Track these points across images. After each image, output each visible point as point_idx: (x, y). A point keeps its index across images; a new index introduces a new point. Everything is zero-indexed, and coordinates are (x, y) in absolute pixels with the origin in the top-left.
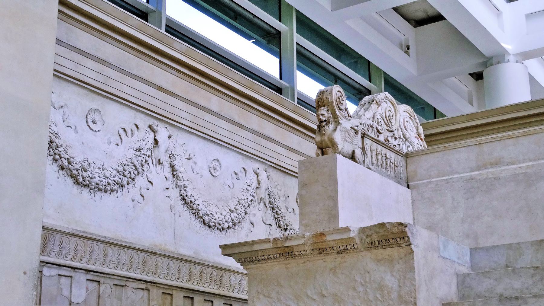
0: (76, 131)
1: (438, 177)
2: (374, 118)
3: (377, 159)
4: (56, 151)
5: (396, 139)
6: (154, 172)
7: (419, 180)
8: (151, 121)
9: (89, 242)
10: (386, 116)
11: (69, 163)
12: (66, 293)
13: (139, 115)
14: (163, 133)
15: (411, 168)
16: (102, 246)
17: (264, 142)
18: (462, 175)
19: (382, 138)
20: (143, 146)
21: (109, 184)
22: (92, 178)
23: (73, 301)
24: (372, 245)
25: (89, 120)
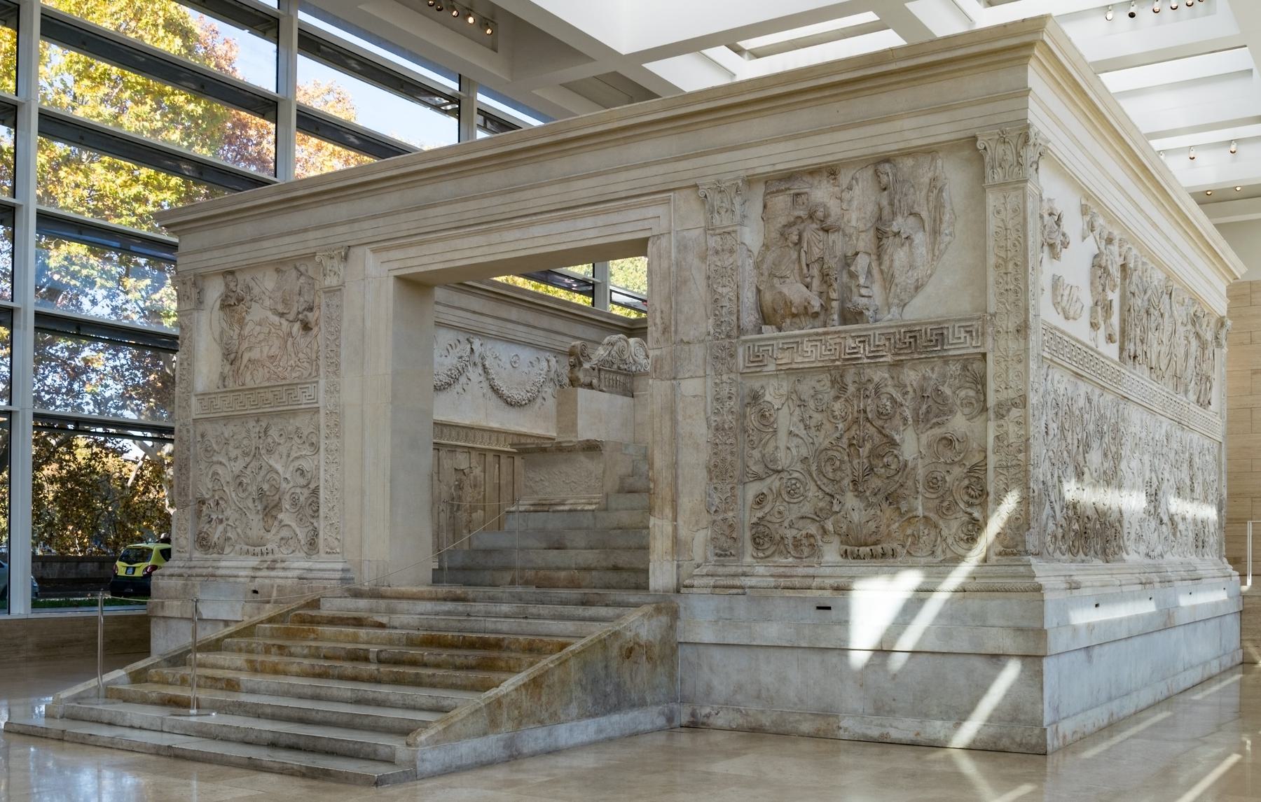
14: (477, 343)
17: (553, 336)
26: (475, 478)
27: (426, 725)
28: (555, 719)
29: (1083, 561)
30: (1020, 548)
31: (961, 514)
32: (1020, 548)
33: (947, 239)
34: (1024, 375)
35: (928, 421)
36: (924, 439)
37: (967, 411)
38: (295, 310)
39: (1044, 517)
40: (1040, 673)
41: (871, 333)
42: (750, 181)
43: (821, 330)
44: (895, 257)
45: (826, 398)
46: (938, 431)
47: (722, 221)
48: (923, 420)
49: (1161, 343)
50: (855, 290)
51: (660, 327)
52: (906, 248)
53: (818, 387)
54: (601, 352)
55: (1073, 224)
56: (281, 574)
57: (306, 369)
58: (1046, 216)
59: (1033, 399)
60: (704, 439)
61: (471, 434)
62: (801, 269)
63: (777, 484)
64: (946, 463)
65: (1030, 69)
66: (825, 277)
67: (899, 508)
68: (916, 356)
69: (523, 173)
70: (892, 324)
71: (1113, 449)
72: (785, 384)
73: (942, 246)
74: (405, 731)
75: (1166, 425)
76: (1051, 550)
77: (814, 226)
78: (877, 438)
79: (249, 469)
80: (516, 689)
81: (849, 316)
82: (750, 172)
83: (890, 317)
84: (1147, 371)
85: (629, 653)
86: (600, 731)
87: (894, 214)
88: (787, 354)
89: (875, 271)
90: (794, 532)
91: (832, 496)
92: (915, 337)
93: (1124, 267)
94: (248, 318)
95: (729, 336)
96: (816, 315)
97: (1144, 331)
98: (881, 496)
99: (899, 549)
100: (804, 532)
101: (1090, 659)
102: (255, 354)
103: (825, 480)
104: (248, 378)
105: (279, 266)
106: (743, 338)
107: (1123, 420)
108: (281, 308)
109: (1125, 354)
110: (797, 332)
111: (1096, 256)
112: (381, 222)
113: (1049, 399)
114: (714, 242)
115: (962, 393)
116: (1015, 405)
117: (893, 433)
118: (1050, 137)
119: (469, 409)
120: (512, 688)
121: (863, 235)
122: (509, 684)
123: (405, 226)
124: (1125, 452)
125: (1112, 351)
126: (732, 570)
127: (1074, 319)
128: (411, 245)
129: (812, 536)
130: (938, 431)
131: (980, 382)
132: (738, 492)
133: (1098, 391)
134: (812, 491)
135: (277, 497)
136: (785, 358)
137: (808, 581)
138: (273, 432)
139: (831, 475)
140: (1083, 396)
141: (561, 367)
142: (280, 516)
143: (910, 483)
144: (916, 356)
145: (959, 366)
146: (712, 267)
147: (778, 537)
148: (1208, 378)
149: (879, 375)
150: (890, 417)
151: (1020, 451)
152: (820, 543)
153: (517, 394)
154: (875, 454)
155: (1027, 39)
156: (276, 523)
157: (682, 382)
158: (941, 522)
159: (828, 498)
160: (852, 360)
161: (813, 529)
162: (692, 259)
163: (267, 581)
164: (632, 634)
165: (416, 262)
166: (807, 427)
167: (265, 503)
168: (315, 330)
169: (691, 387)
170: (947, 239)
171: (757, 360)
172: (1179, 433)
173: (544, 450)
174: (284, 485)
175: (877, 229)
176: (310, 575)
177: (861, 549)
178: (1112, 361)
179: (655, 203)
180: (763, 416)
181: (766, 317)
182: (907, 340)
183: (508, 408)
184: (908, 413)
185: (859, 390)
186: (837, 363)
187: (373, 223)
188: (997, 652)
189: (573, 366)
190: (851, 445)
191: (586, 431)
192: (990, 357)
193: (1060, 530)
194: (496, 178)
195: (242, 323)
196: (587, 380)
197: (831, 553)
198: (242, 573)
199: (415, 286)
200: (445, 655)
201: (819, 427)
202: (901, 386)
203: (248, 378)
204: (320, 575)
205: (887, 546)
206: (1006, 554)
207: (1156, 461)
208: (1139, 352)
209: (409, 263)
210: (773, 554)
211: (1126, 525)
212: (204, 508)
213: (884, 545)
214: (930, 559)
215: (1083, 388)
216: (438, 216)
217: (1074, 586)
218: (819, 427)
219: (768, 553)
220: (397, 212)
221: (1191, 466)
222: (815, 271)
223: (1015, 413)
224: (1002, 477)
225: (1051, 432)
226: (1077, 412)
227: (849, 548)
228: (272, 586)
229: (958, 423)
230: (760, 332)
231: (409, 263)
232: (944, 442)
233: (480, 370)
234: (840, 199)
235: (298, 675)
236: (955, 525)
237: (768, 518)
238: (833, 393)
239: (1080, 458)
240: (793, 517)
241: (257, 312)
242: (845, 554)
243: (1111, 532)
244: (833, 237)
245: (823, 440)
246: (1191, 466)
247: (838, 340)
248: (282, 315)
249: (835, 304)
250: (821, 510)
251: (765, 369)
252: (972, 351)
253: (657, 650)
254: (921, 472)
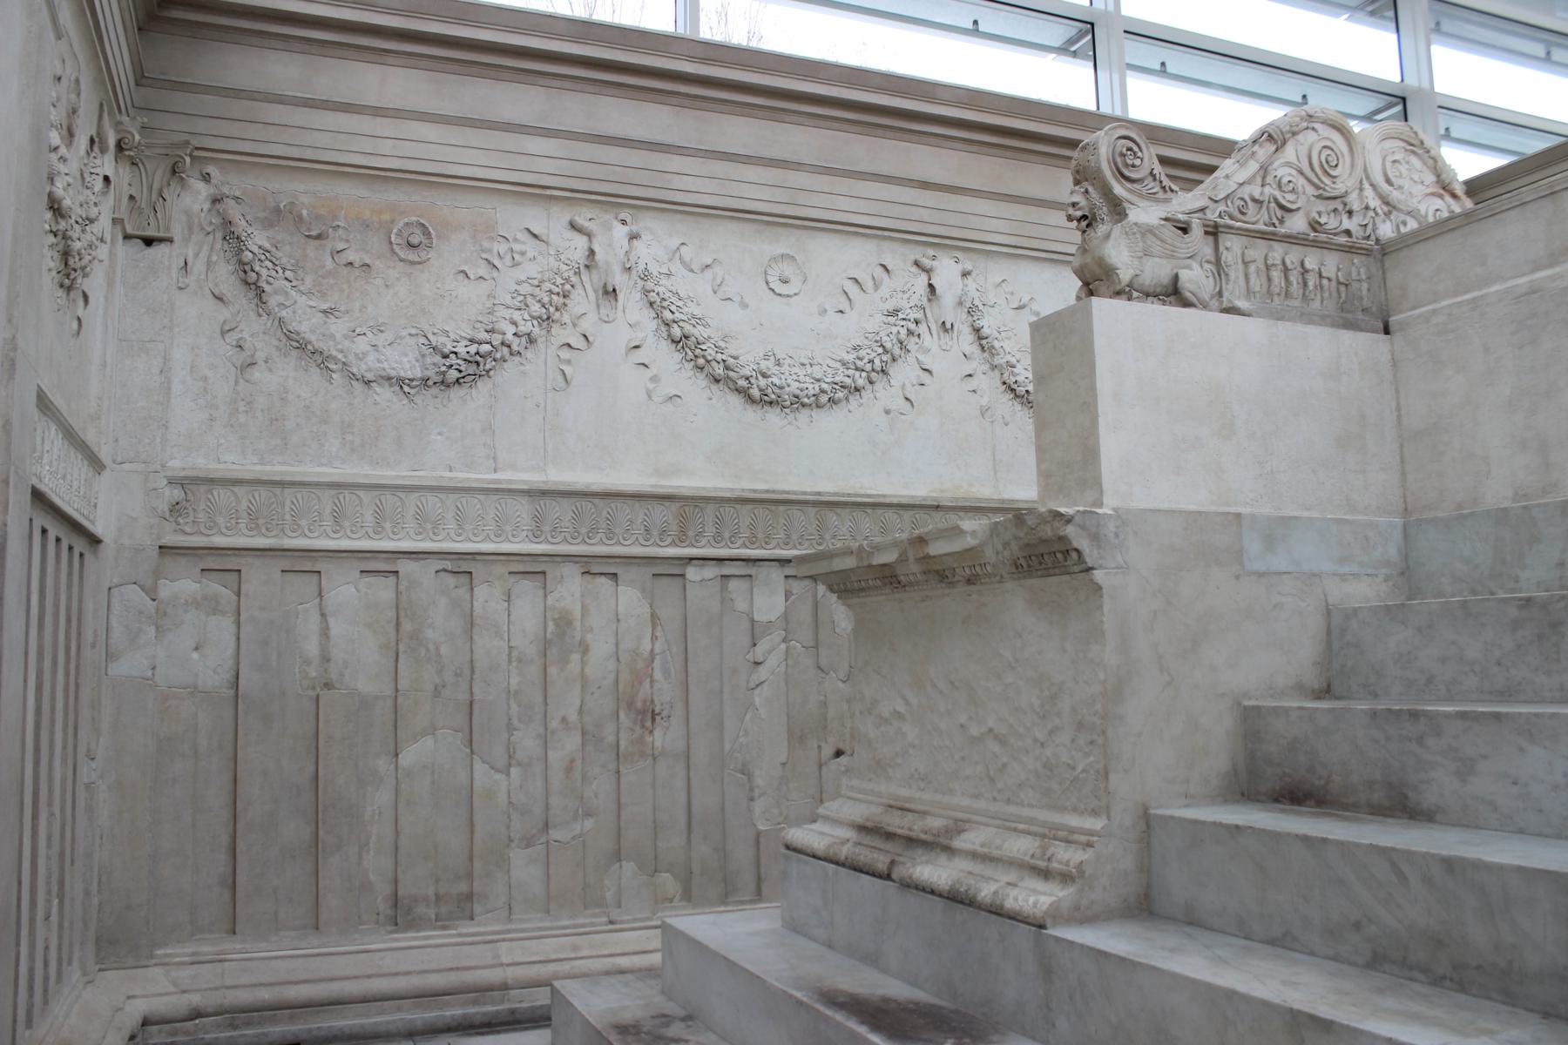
0: (744, 305)
1: (1456, 294)
2: (1264, 178)
3: (1269, 280)
4: (698, 352)
5: (1350, 213)
6: (935, 349)
7: (1414, 308)
8: (916, 253)
9: (782, 508)
10: (1311, 164)
11: (727, 368)
12: (741, 605)
13: (886, 245)
14: (947, 271)
15: (1394, 279)
16: (812, 511)
18: (1510, 283)
19: (1297, 224)
20: (904, 304)
21: (823, 391)
22: (781, 388)
23: (756, 618)
25: (770, 279)
173: (941, 574)
196: (1156, 271)
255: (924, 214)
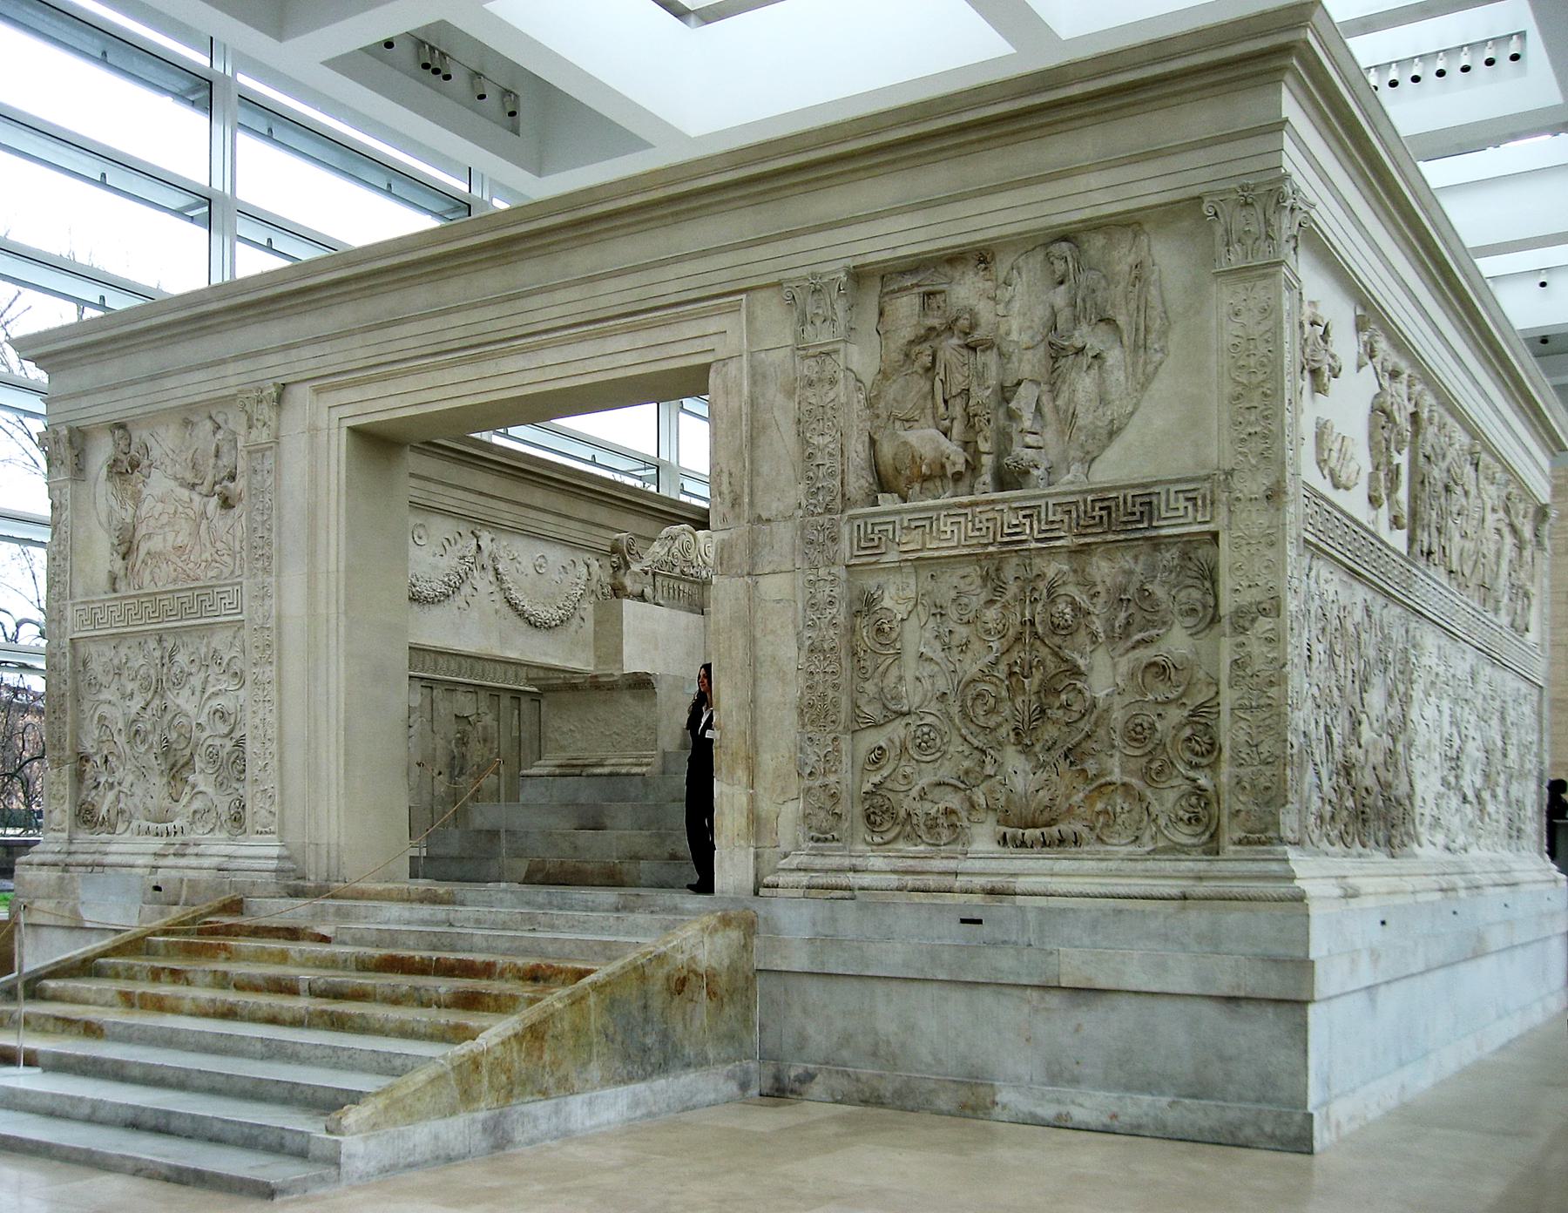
13: (462, 523)
17: (595, 530)
24: (630, 687)
26: (485, 728)
27: (355, 1097)
28: (566, 1087)
29: (1360, 856)
30: (1271, 834)
31: (1178, 781)
32: (1271, 834)
33: (1157, 357)
34: (1276, 567)
35: (1128, 636)
36: (1124, 665)
37: (1190, 621)
38: (209, 479)
39: (1306, 787)
40: (1303, 1027)
41: (1042, 502)
42: (858, 276)
43: (965, 499)
44: (1080, 387)
45: (976, 602)
46: (1146, 654)
47: (822, 336)
48: (1120, 635)
49: (1464, 536)
50: (1016, 437)
51: (728, 499)
52: (1094, 371)
53: (962, 585)
54: (657, 550)
55: (1346, 345)
56: (194, 862)
57: (224, 564)
58: (1307, 327)
59: (1292, 604)
60: (793, 665)
61: (478, 666)
62: (935, 407)
63: (902, 732)
64: (1156, 702)
65: (1285, 90)
66: (969, 419)
67: (1084, 770)
68: (1110, 537)
69: (528, 272)
70: (1073, 488)
71: (1401, 688)
72: (912, 581)
73: (1150, 368)
74: (329, 1104)
75: (1471, 655)
76: (1315, 837)
77: (955, 341)
78: (1051, 662)
79: (149, 711)
80: (503, 1043)
81: (1008, 478)
82: (859, 261)
83: (1071, 479)
84: (1444, 580)
85: (680, 985)
86: (636, 1104)
87: (1076, 320)
88: (917, 534)
89: (1047, 409)
90: (927, 806)
91: (984, 752)
92: (1108, 508)
93: (1414, 416)
94: (146, 492)
95: (828, 510)
96: (958, 477)
97: (1441, 516)
98: (1058, 753)
99: (1085, 833)
100: (942, 806)
101: (1373, 1001)
102: (156, 544)
103: (973, 728)
104: (147, 577)
105: (187, 418)
106: (851, 512)
107: (1414, 647)
108: (190, 477)
109: (1416, 548)
110: (930, 502)
111: (1376, 396)
112: (327, 348)
113: (1314, 606)
114: (809, 368)
115: (1183, 595)
116: (1264, 612)
117: (1076, 656)
118: (1312, 198)
119: (471, 630)
120: (498, 1040)
121: (1029, 355)
122: (494, 1031)
123: (360, 353)
124: (1417, 693)
125: (1398, 540)
126: (834, 862)
127: (1347, 488)
128: (370, 380)
129: (953, 812)
130: (1146, 654)
131: (1209, 575)
132: (845, 744)
133: (1381, 600)
134: (956, 746)
135: (187, 752)
136: (913, 541)
137: (948, 881)
138: (182, 658)
139: (982, 721)
140: (1360, 606)
141: (601, 572)
142: (191, 778)
143: (1101, 732)
144: (1110, 537)
145: (1175, 552)
146: (805, 407)
147: (902, 813)
148: (1526, 595)
149: (1053, 568)
150: (1070, 631)
151: (1271, 684)
152: (966, 823)
153: (544, 612)
154: (1048, 689)
155: (1282, 39)
156: (188, 789)
157: (760, 579)
158: (1148, 793)
159: (977, 754)
160: (1013, 545)
161: (953, 801)
162: (773, 395)
163: (174, 873)
164: (686, 957)
165: (379, 405)
166: (947, 648)
167: (171, 760)
168: (237, 510)
169: (774, 587)
170: (1157, 357)
171: (871, 545)
172: (1488, 669)
173: (575, 687)
174: (196, 733)
175: (1050, 344)
176: (234, 864)
177: (1027, 832)
178: (1400, 555)
179: (720, 312)
180: (880, 631)
181: (883, 483)
182: (1097, 513)
183: (533, 631)
184: (1098, 625)
185: (1023, 590)
186: (991, 549)
187: (316, 350)
188: (1237, 994)
189: (616, 569)
190: (1011, 674)
191: (633, 662)
192: (1224, 539)
193: (1328, 808)
194: (492, 281)
195: (137, 499)
196: (637, 588)
197: (983, 838)
198: (140, 861)
199: (377, 443)
200: (404, 982)
201: (964, 647)
202: (1087, 584)
203: (147, 577)
204: (247, 863)
205: (1066, 827)
206: (1249, 843)
207: (1458, 710)
208: (1435, 548)
209: (369, 407)
210: (895, 839)
211: (1418, 802)
212: (88, 767)
213: (1063, 827)
214: (1131, 848)
215: (1361, 593)
216: (408, 337)
217: (1350, 894)
218: (964, 647)
219: (888, 837)
220: (351, 333)
221: (1503, 719)
222: (957, 408)
223: (1264, 624)
224: (1243, 724)
225: (1315, 657)
226: (1351, 629)
227: (1009, 831)
228: (182, 881)
229: (1177, 642)
230: (875, 503)
231: (369, 407)
232: (1154, 670)
233: (491, 573)
234: (994, 299)
235: (192, 1015)
236: (1171, 796)
237: (888, 784)
238: (984, 597)
239: (1356, 700)
240: (924, 781)
241: (159, 485)
242: (1003, 841)
243: (1397, 813)
244: (981, 358)
245: (971, 666)
246: (1503, 719)
247: (991, 515)
248: (193, 486)
249: (987, 461)
250: (967, 773)
251: (885, 559)
252: (1195, 528)
253: (723, 981)
254: (1118, 716)
255: (480, 509)
